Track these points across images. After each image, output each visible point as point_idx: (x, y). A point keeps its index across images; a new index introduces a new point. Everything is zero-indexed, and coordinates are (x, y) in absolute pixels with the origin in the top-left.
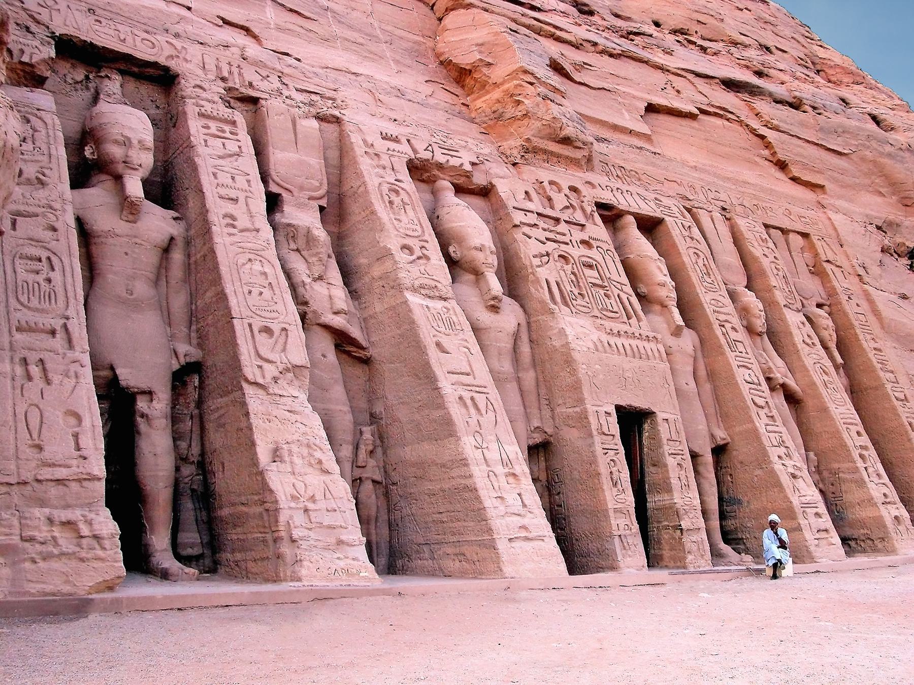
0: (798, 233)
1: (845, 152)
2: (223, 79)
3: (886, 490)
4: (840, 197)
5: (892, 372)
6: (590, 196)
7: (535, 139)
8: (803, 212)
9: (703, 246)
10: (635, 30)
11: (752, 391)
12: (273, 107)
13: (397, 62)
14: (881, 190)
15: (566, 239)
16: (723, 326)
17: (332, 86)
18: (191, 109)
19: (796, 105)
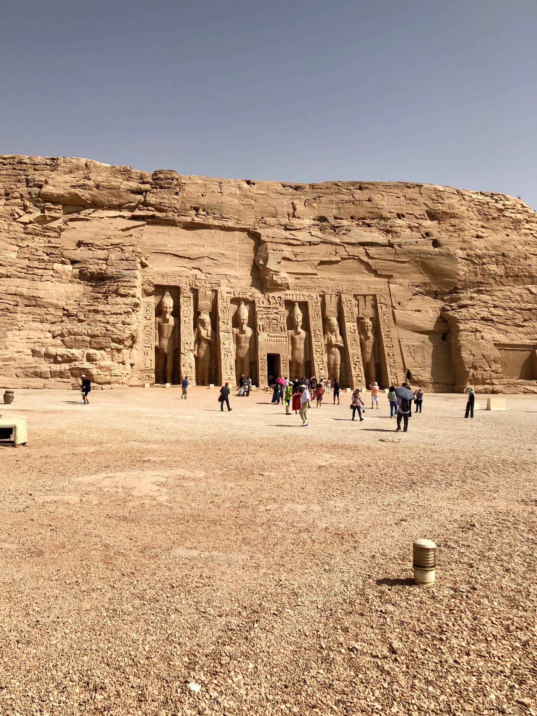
2: (190, 285)
4: (399, 278)
6: (284, 297)
8: (376, 287)
9: (319, 308)
10: (337, 225)
12: (201, 290)
13: (240, 266)
14: (423, 272)
17: (218, 280)
18: (181, 296)
19: (391, 245)
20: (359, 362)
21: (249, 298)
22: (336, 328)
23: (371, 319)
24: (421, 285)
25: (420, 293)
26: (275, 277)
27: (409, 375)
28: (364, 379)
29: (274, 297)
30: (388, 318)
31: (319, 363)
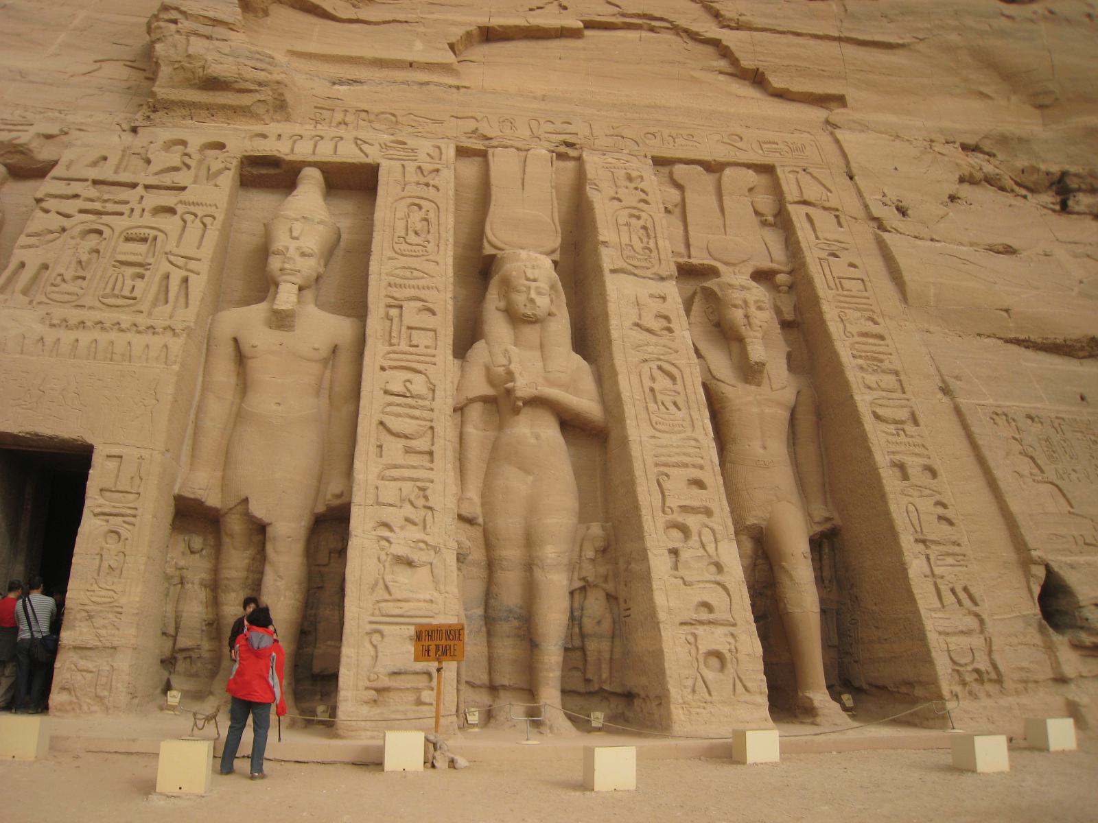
0: (748, 166)
1: (901, 41)
3: (715, 597)
5: (896, 373)
7: (163, 90)
11: (388, 409)
15: (125, 208)
16: (401, 307)
20: (708, 512)
21: (34, 145)
22: (543, 302)
23: (761, 276)
24: (986, 145)
25: (989, 180)
26: (197, 46)
27: (1055, 603)
28: (750, 646)
29: (184, 143)
30: (853, 272)
31: (394, 516)
